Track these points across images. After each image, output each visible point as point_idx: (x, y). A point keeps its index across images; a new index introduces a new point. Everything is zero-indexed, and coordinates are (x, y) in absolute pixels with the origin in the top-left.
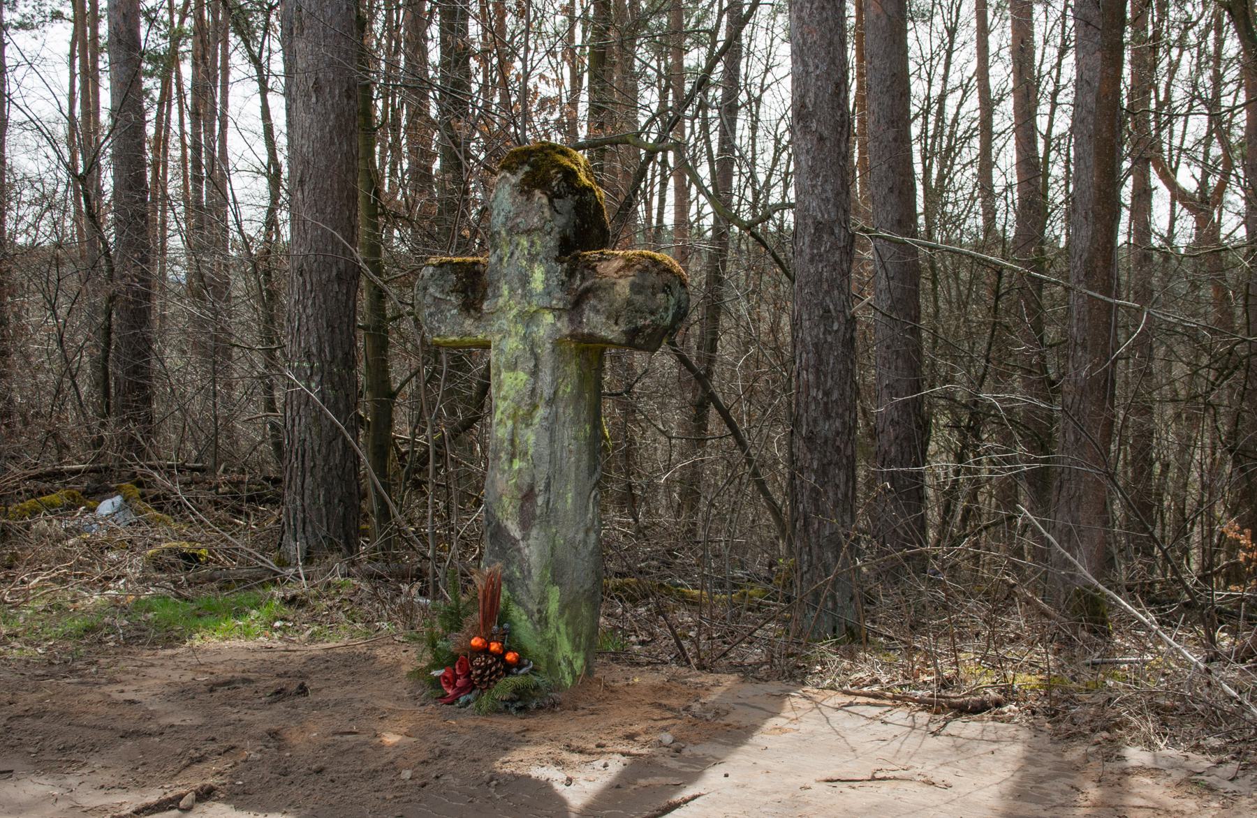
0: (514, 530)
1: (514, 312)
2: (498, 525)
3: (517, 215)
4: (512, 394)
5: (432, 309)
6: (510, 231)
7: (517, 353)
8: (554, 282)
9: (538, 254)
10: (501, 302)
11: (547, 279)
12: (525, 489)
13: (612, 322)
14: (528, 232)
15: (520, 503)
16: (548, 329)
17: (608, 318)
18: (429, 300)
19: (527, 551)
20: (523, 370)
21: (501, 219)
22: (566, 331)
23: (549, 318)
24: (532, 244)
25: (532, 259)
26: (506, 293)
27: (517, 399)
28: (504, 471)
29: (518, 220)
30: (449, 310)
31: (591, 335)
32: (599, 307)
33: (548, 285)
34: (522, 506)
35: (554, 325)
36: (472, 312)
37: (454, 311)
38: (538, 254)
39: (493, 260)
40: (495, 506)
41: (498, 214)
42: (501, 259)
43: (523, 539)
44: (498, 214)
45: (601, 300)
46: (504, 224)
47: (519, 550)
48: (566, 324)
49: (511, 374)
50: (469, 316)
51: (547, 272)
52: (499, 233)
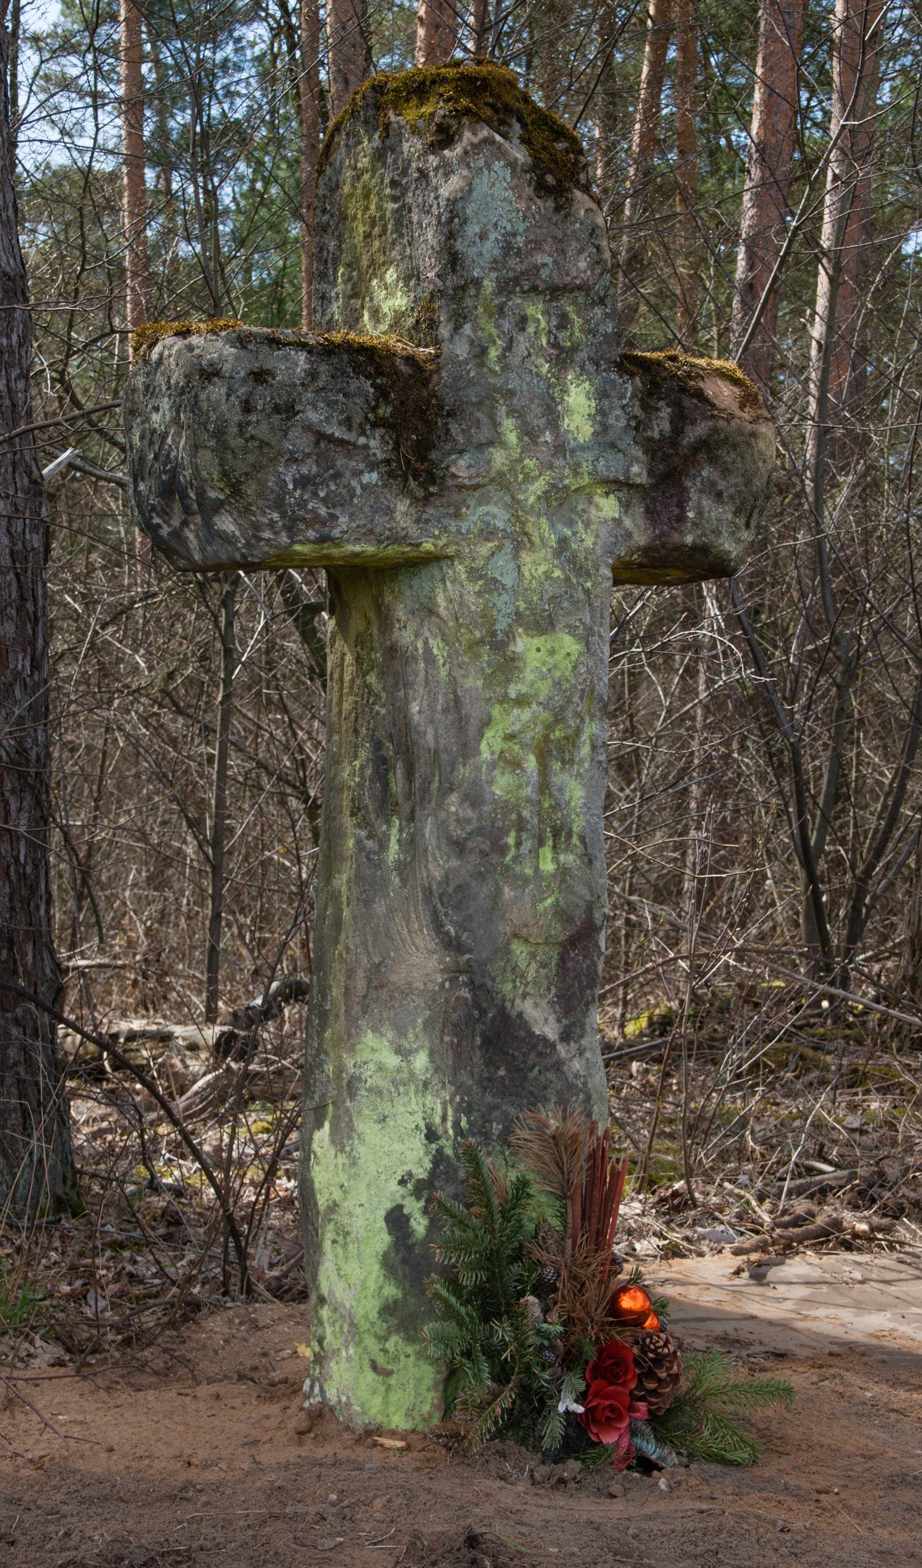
0: (544, 1023)
1: (538, 486)
2: (503, 1015)
3: (537, 245)
4: (544, 689)
5: (309, 468)
6: (506, 287)
7: (550, 590)
8: (618, 420)
9: (575, 349)
10: (499, 458)
11: (602, 412)
12: (579, 915)
13: (741, 521)
14: (555, 292)
15: (555, 954)
16: (603, 532)
17: (736, 513)
18: (299, 441)
19: (577, 1065)
20: (571, 630)
21: (490, 248)
22: (641, 539)
23: (608, 506)
24: (564, 322)
25: (562, 357)
26: (512, 438)
27: (559, 700)
28: (526, 880)
29: (540, 259)
30: (358, 474)
31: (703, 549)
32: (721, 485)
33: (605, 428)
34: (563, 960)
35: (618, 522)
36: (412, 483)
37: (372, 477)
38: (575, 349)
39: (461, 350)
40: (496, 967)
41: (483, 236)
42: (481, 352)
43: (566, 1037)
44: (483, 236)
45: (726, 471)
46: (495, 265)
47: (558, 1066)
48: (641, 521)
49: (537, 642)
50: (404, 490)
51: (602, 394)
52: (477, 283)
